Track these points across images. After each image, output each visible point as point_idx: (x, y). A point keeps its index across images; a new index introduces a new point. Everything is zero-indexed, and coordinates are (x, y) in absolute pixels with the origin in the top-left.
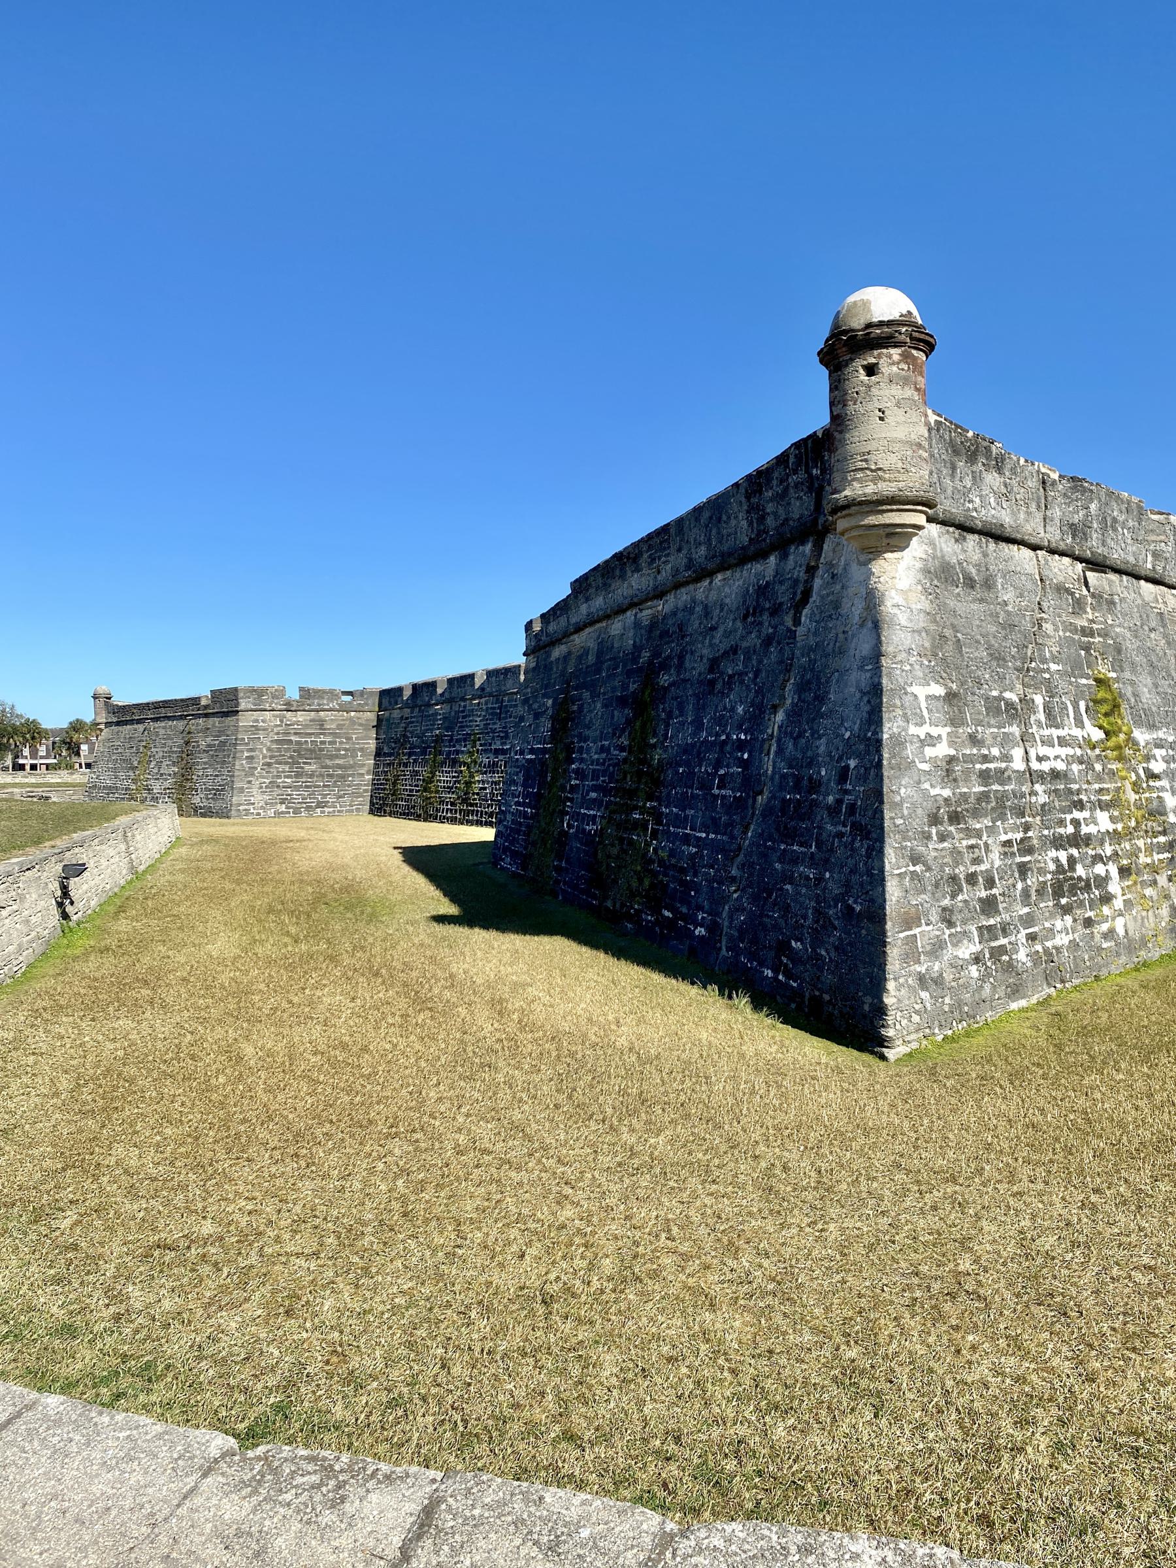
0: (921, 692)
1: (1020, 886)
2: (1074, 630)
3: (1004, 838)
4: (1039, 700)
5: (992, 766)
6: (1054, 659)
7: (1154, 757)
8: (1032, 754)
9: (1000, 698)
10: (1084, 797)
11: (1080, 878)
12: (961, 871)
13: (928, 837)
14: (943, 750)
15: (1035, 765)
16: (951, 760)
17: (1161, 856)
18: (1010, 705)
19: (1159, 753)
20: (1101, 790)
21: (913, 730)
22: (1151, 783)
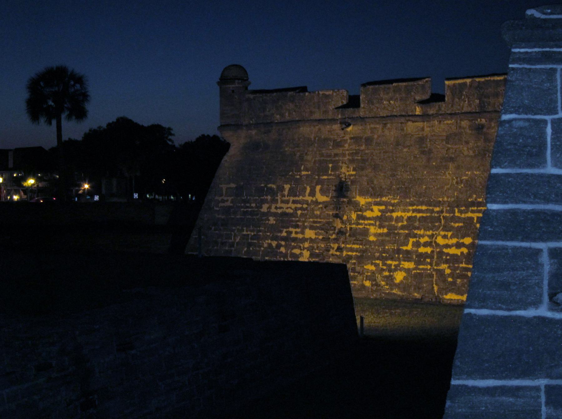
0: (224, 187)
1: (245, 249)
2: (330, 156)
3: (245, 233)
4: (287, 187)
5: (250, 210)
6: (306, 169)
7: (372, 210)
8: (273, 206)
9: (266, 186)
10: (300, 224)
11: (281, 252)
12: (220, 240)
13: (211, 229)
14: (229, 204)
15: (273, 210)
16: (230, 207)
17: (350, 253)
18: (271, 189)
19: (376, 208)
20: (314, 222)
21: (217, 198)
22: (361, 221)
